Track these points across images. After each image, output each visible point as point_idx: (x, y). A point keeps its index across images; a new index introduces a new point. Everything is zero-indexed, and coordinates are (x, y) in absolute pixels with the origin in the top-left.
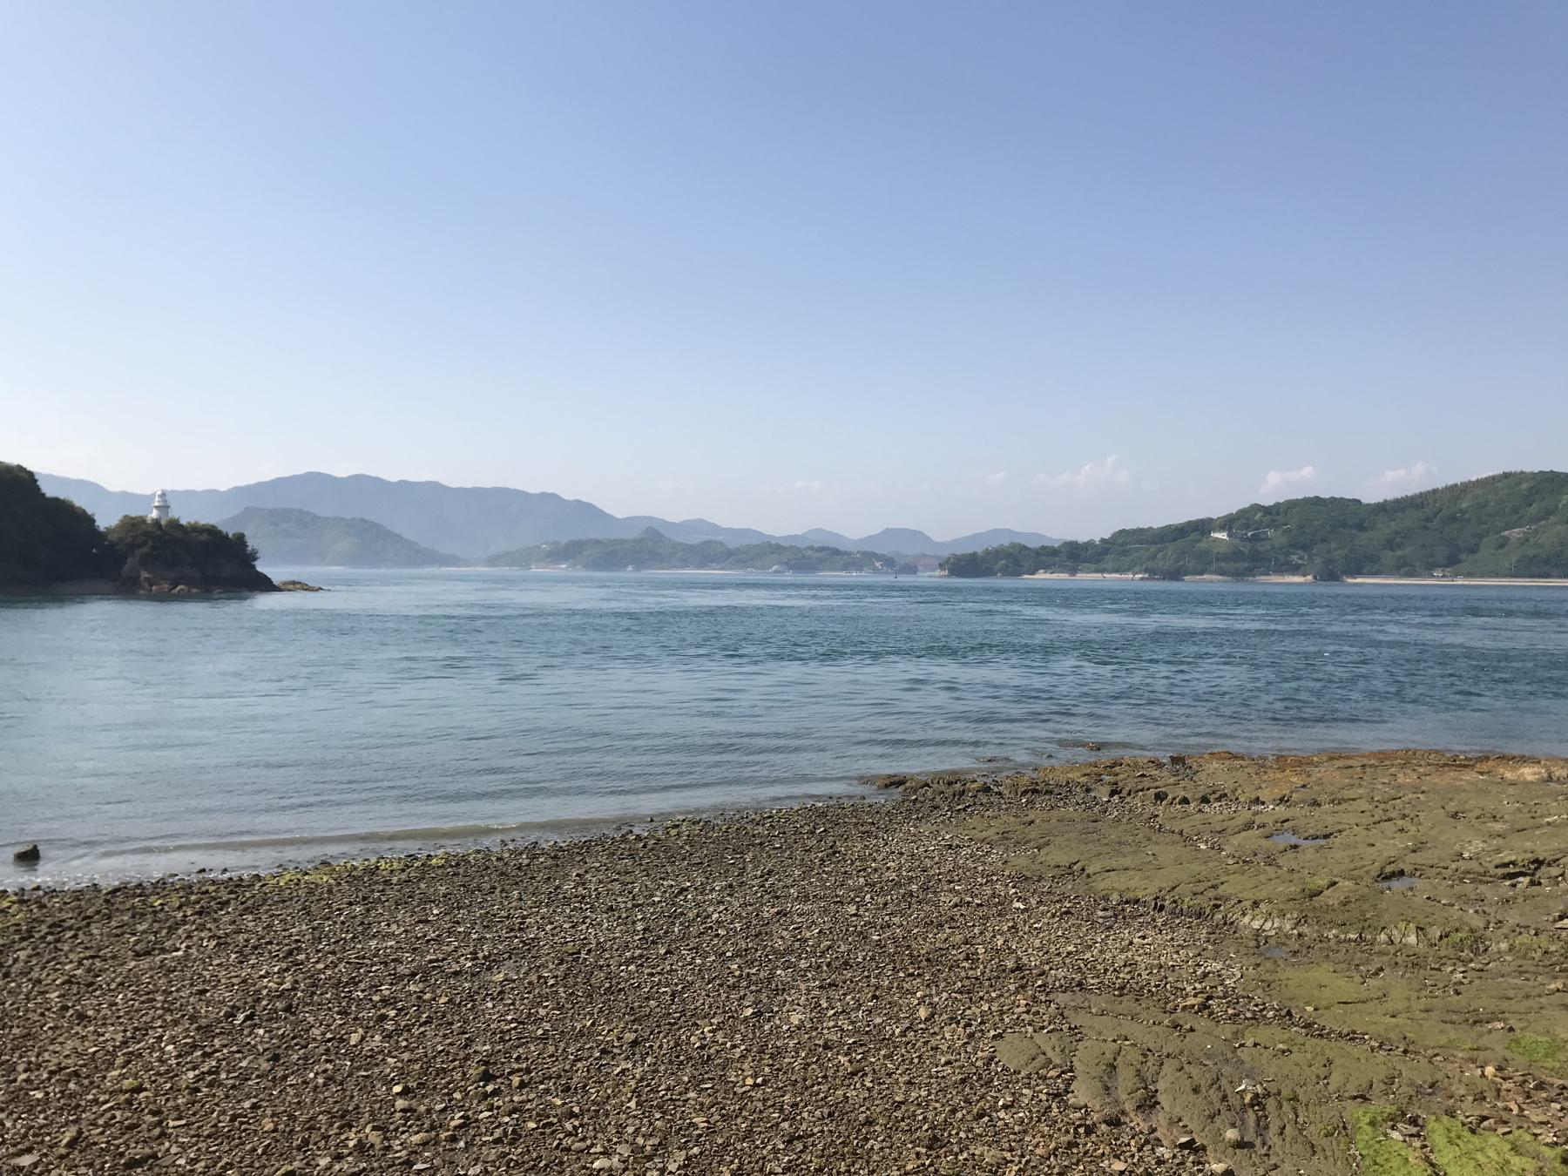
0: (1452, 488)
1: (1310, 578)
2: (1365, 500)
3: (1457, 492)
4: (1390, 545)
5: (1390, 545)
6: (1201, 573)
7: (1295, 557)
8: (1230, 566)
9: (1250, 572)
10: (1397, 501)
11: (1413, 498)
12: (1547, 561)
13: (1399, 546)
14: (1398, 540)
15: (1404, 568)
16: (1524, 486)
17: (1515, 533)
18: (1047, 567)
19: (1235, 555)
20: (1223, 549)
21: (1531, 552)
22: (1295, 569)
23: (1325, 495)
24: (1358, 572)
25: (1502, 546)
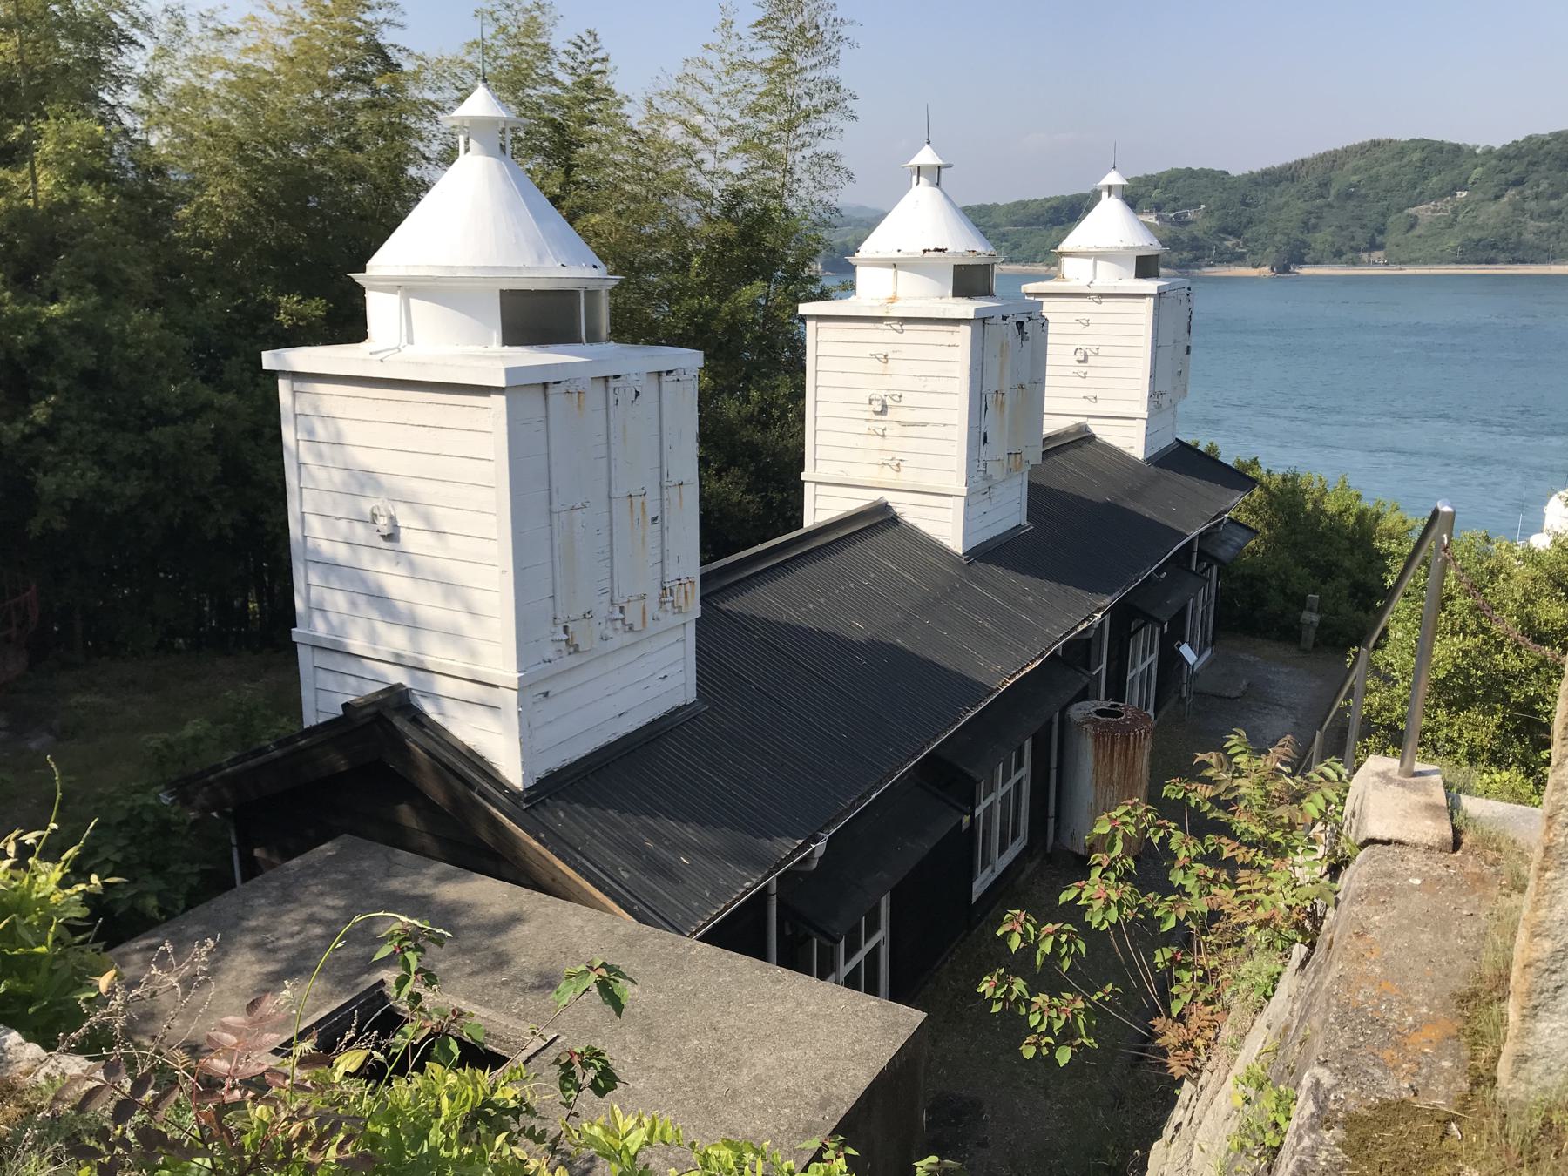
0: (1322, 157)
1: (1265, 271)
2: (1235, 171)
3: (1333, 160)
4: (1307, 227)
5: (1307, 227)
7: (1229, 244)
9: (1194, 263)
10: (1265, 173)
11: (1282, 169)
12: (1494, 246)
13: (1315, 228)
14: (1313, 221)
15: (1337, 256)
16: (1416, 156)
17: (1424, 211)
21: (1475, 235)
22: (1238, 259)
23: (1196, 168)
24: (1301, 262)
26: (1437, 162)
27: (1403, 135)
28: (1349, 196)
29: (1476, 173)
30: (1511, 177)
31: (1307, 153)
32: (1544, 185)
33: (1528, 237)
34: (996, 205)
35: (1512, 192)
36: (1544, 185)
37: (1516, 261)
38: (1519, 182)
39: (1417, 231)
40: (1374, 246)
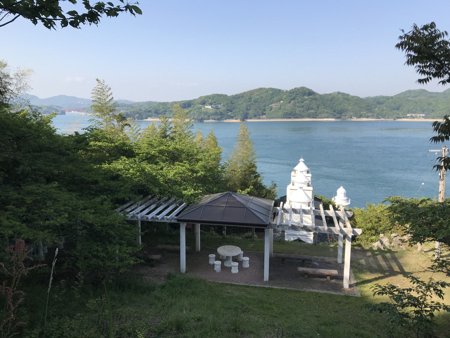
2: (229, 95)
3: (251, 93)
4: (247, 109)
5: (247, 109)
6: (209, 119)
7: (229, 114)
8: (216, 117)
10: (236, 95)
12: (290, 114)
14: (248, 108)
15: (255, 116)
16: (271, 92)
17: (273, 105)
18: (151, 116)
19: (216, 114)
20: (211, 111)
21: (286, 112)
22: (232, 117)
24: (247, 118)
25: (271, 109)
26: (275, 94)
27: (267, 87)
28: (256, 101)
29: (284, 97)
30: (292, 97)
31: (246, 91)
32: (300, 99)
33: (297, 112)
34: (168, 102)
35: (293, 101)
36: (300, 99)
37: (295, 118)
38: (294, 99)
39: (273, 110)
40: (263, 114)
